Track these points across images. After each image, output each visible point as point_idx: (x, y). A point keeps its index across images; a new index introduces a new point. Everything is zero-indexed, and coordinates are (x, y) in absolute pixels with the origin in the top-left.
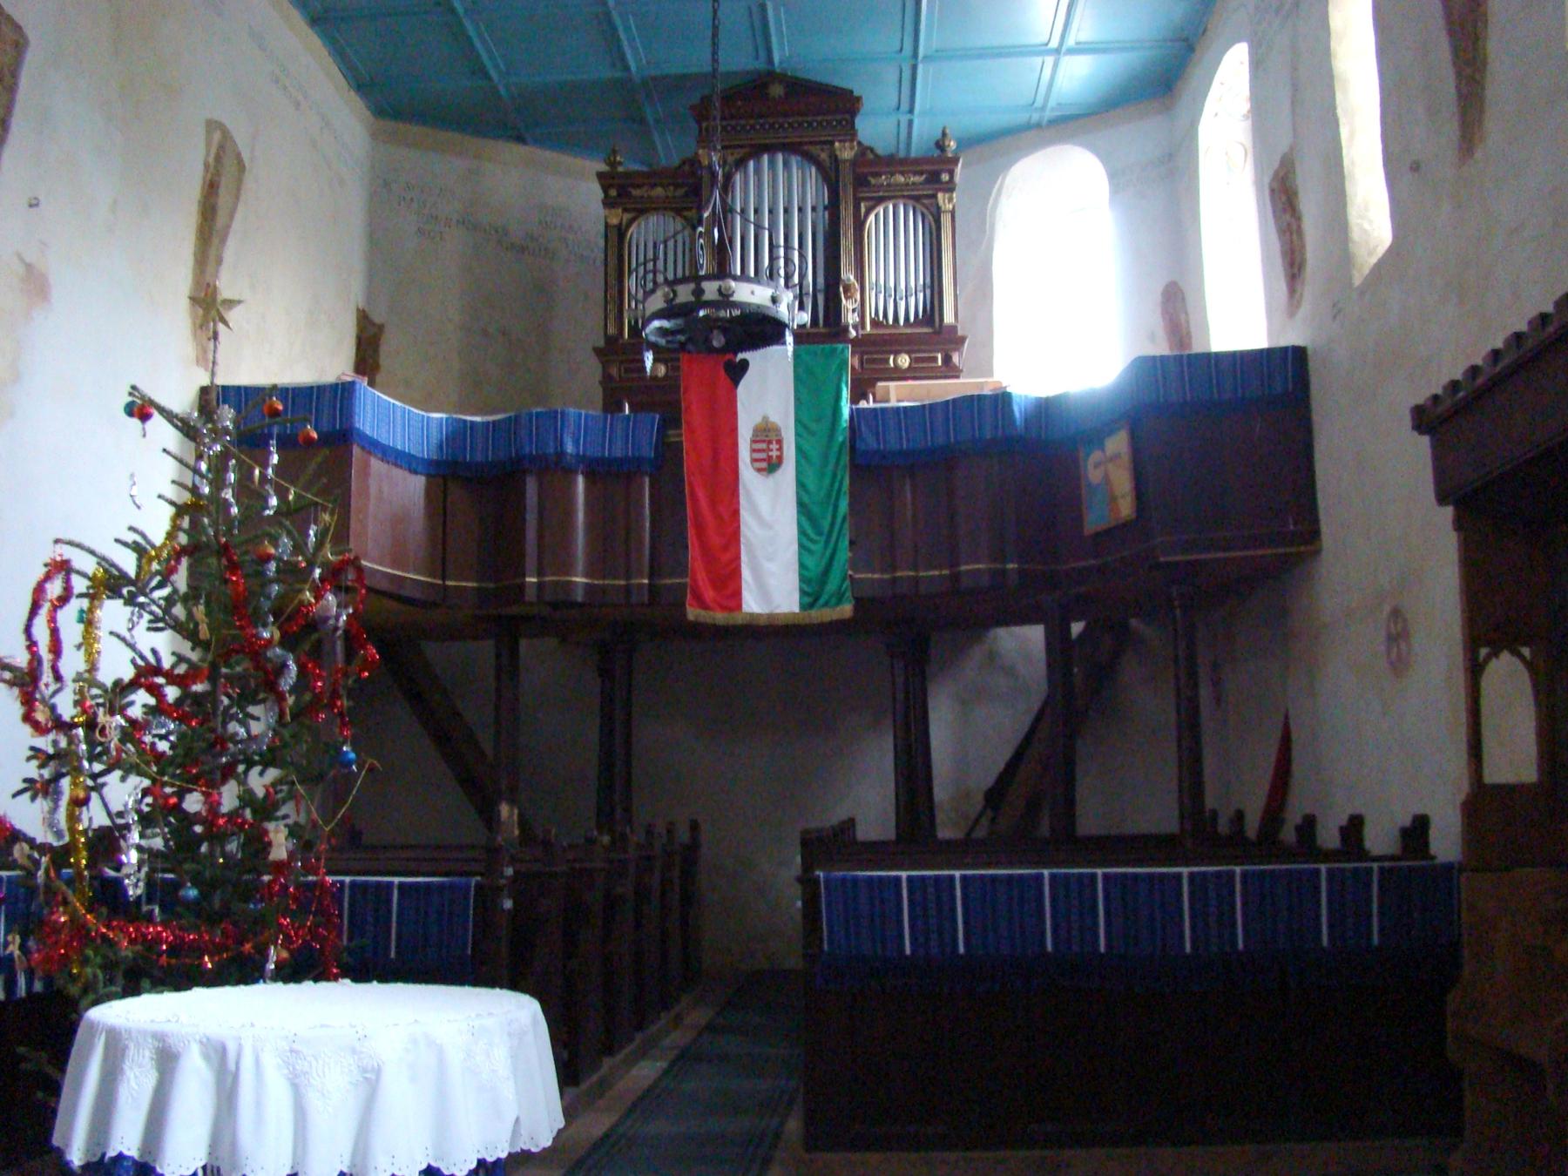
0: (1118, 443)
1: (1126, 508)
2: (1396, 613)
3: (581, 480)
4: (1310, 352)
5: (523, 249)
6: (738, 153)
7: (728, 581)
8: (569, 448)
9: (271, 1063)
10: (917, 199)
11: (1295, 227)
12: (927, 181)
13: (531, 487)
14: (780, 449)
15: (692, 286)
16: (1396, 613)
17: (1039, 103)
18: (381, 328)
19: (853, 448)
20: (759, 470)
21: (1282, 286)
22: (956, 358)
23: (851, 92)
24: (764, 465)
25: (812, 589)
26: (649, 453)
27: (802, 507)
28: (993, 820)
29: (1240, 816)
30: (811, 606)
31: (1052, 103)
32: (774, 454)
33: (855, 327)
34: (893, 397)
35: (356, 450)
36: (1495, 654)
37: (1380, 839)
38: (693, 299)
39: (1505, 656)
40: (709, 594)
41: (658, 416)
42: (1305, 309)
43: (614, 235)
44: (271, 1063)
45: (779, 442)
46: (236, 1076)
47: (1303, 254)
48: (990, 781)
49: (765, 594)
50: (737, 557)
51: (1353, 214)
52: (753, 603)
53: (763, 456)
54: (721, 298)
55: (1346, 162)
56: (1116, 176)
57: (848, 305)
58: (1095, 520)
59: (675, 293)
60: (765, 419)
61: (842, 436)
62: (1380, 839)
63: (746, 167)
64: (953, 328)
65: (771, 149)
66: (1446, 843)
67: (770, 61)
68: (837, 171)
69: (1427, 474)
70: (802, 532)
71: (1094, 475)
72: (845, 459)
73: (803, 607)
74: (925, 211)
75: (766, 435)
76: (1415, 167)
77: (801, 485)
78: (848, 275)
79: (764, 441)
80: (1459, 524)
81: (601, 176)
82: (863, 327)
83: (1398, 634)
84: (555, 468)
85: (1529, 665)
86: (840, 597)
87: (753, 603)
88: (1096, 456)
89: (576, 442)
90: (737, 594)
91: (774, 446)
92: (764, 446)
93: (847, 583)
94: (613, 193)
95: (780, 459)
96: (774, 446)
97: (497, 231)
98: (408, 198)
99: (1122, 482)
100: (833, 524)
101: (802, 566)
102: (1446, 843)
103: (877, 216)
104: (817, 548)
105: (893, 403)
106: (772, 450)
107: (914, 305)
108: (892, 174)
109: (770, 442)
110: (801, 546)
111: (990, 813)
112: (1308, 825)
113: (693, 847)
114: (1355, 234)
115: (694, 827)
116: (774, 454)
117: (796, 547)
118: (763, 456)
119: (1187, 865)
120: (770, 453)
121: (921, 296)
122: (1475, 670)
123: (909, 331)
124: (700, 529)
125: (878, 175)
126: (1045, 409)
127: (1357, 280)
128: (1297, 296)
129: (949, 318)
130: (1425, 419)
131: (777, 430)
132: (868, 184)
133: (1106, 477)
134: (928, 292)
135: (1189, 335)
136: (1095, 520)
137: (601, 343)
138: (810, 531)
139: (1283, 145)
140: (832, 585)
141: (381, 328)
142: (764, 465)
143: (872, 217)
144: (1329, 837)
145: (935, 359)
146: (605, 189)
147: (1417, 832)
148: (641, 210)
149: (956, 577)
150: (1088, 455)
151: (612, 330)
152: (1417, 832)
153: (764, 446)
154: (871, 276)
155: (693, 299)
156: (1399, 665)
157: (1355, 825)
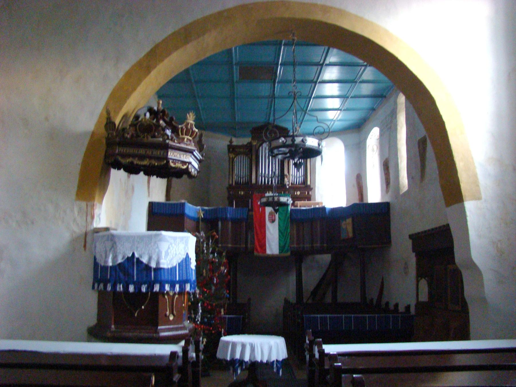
0: (349, 220)
1: (351, 235)
2: (406, 264)
3: (230, 223)
4: (391, 203)
6: (260, 143)
7: (263, 247)
8: (228, 216)
9: (259, 345)
13: (220, 224)
16: (406, 264)
19: (291, 218)
21: (385, 186)
22: (310, 193)
23: (288, 129)
25: (282, 248)
26: (245, 217)
27: (280, 231)
29: (372, 299)
30: (281, 253)
31: (333, 128)
34: (299, 206)
35: (185, 218)
36: (421, 279)
37: (401, 309)
39: (423, 279)
40: (259, 249)
42: (390, 193)
43: (231, 160)
44: (259, 345)
46: (254, 347)
47: (390, 181)
49: (271, 249)
50: (265, 241)
51: (400, 179)
52: (268, 252)
55: (399, 168)
56: (346, 146)
57: (286, 180)
58: (343, 236)
61: (288, 215)
62: (401, 309)
64: (310, 186)
66: (413, 310)
67: (269, 120)
69: (410, 247)
70: (279, 236)
71: (343, 226)
72: (289, 220)
73: (279, 252)
76: (412, 178)
77: (279, 225)
78: (286, 172)
80: (416, 256)
83: (406, 267)
84: (224, 220)
85: (428, 281)
86: (287, 251)
87: (268, 252)
88: (344, 223)
89: (230, 215)
90: (265, 250)
91: (274, 216)
93: (289, 247)
99: (350, 229)
100: (286, 234)
101: (279, 243)
102: (413, 310)
104: (283, 240)
105: (299, 208)
107: (301, 179)
110: (279, 239)
112: (387, 304)
114: (401, 183)
117: (278, 239)
119: (368, 314)
122: (418, 282)
123: (300, 186)
124: (257, 234)
126: (333, 210)
127: (401, 193)
128: (388, 190)
129: (309, 183)
130: (411, 237)
133: (346, 228)
135: (362, 187)
136: (343, 236)
137: (227, 186)
138: (282, 236)
139: (387, 156)
140: (286, 248)
144: (391, 307)
147: (408, 308)
148: (237, 154)
149: (312, 247)
151: (231, 182)
152: (408, 308)
154: (291, 173)
156: (406, 273)
157: (396, 305)
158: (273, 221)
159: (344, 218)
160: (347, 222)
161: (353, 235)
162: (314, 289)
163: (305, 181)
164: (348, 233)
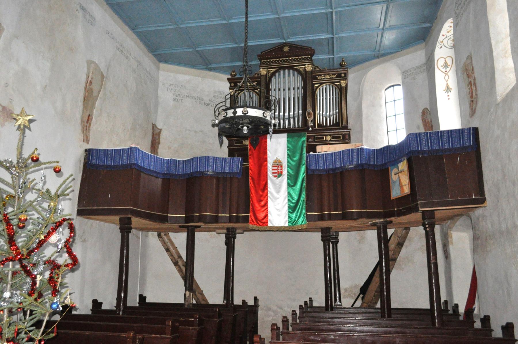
0: (403, 165)
1: (407, 190)
5: (208, 105)
10: (333, 83)
11: (472, 83)
12: (337, 77)
14: (282, 169)
15: (233, 110)
17: (377, 49)
18: (161, 130)
20: (275, 176)
24: (276, 175)
28: (363, 298)
29: (457, 306)
32: (280, 171)
33: (312, 127)
38: (233, 115)
41: (241, 158)
45: (282, 167)
48: (362, 284)
53: (276, 171)
54: (243, 115)
59: (226, 113)
60: (277, 158)
63: (275, 75)
65: (284, 68)
68: (306, 74)
71: (394, 177)
74: (336, 87)
75: (278, 164)
79: (276, 166)
81: (229, 79)
82: (315, 127)
88: (395, 170)
91: (280, 168)
92: (276, 168)
94: (233, 85)
95: (282, 172)
96: (280, 168)
97: (200, 99)
98: (170, 88)
99: (405, 180)
103: (319, 89)
106: (279, 169)
108: (325, 75)
109: (278, 167)
111: (361, 296)
112: (486, 320)
113: (256, 306)
115: (256, 299)
116: (280, 171)
118: (276, 171)
120: (278, 171)
121: (335, 116)
125: (320, 75)
129: (344, 123)
131: (280, 162)
132: (317, 79)
134: (337, 114)
141: (161, 130)
142: (276, 175)
143: (318, 90)
145: (340, 137)
146: (230, 83)
150: (393, 169)
153: (276, 168)
155: (233, 115)
158: (279, 175)
159: (395, 163)
160: (400, 168)
161: (411, 191)
162: (365, 283)
163: (339, 122)
164: (401, 187)
